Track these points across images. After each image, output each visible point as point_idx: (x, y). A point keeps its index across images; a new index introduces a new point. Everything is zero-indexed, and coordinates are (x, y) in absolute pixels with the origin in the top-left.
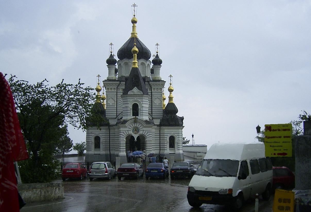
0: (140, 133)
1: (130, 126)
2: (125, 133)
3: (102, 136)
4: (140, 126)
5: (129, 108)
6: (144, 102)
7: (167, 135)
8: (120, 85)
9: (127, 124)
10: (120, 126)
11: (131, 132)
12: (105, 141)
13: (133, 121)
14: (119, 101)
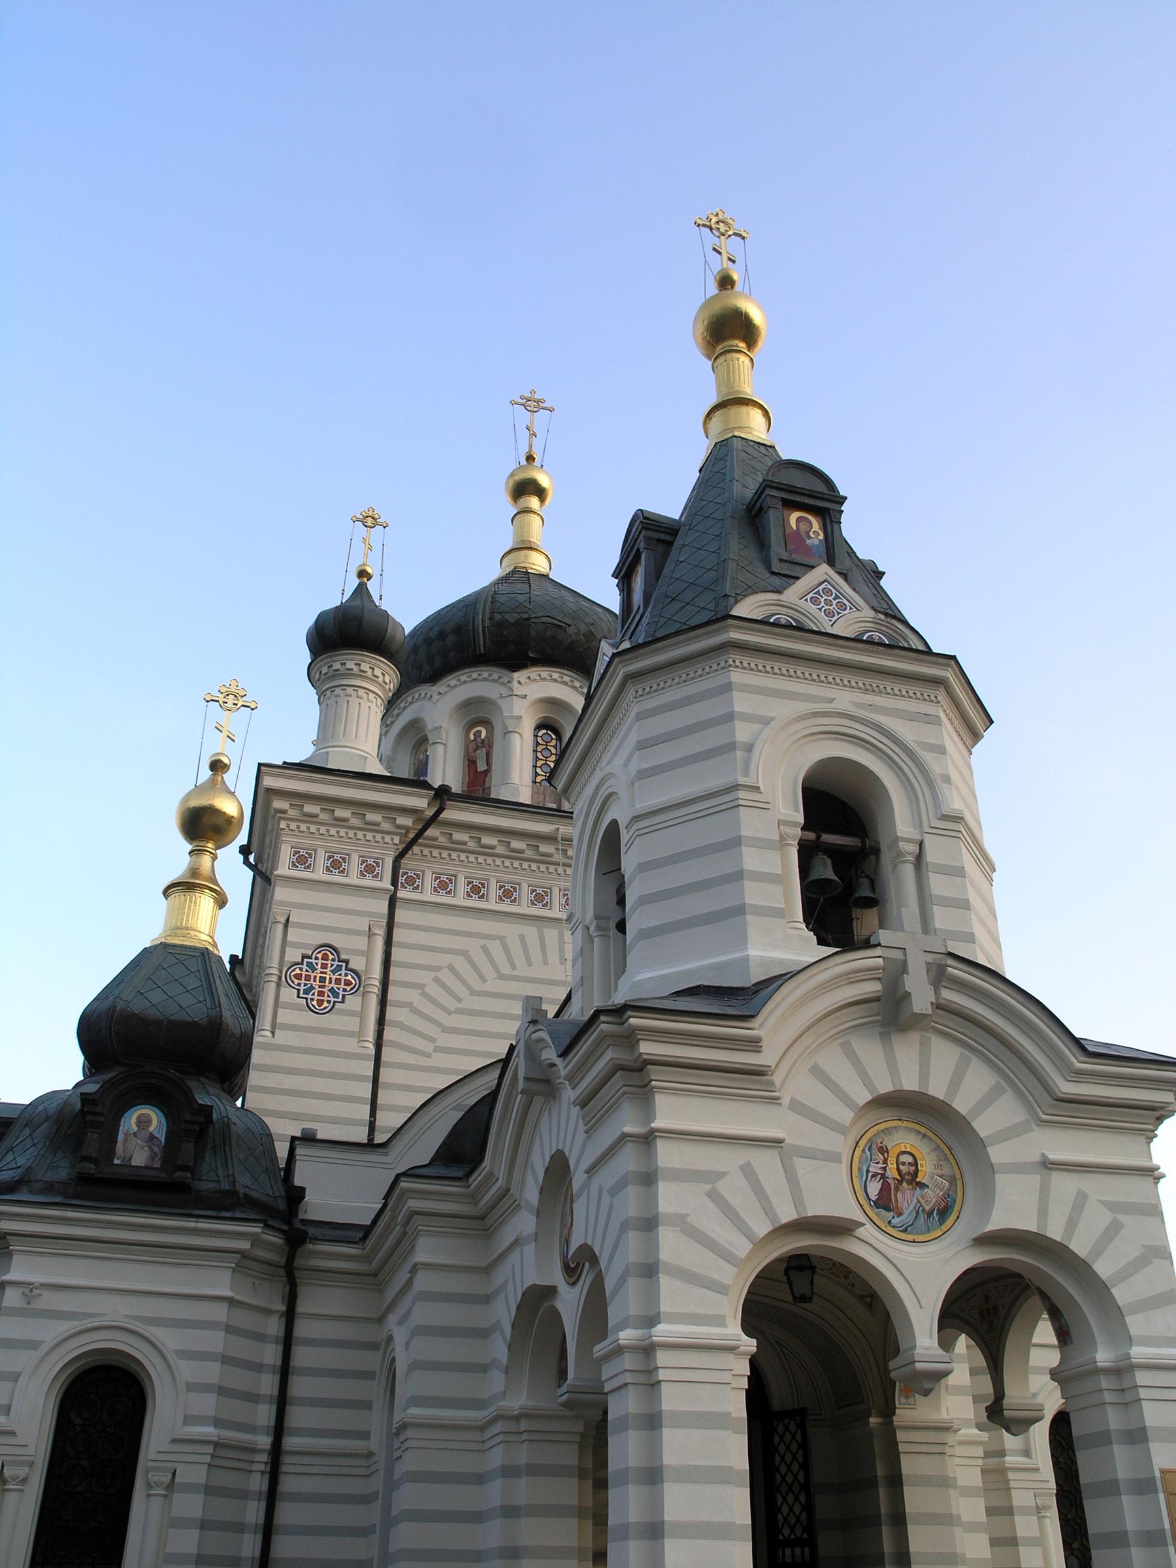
0: (998, 1221)
2: (735, 1190)
3: (183, 1354)
5: (764, 807)
8: (431, 832)
9: (776, 1026)
10: (647, 1048)
11: (832, 1193)
12: (217, 1445)
13: (873, 988)
14: (413, 996)
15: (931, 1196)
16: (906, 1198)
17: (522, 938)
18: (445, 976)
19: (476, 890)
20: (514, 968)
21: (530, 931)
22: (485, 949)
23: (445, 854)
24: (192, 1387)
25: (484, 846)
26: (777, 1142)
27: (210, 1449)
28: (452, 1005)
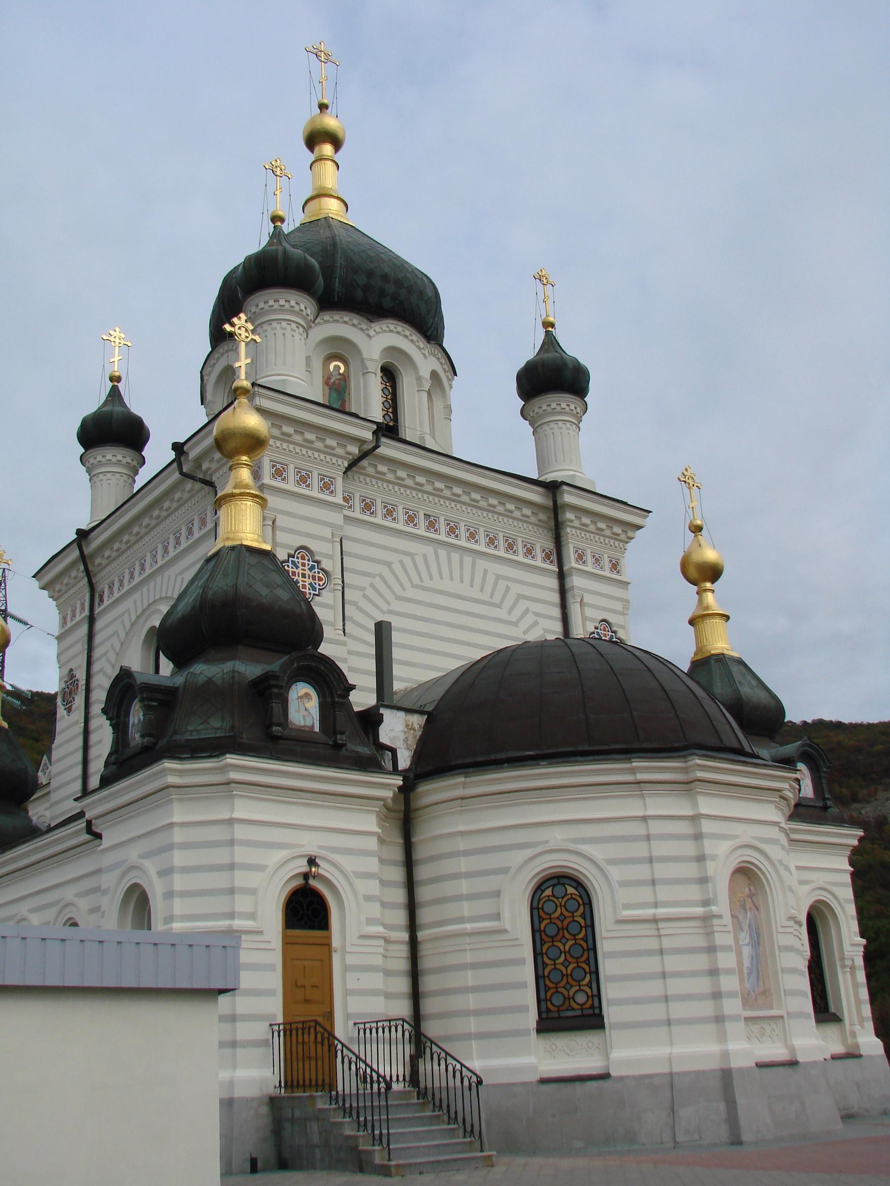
8: (364, 463)
17: (425, 556)
18: (377, 581)
19: (389, 513)
20: (422, 581)
21: (429, 550)
22: (401, 562)
23: (368, 480)
24: (368, 898)
25: (378, 472)
27: (382, 943)
28: (385, 607)
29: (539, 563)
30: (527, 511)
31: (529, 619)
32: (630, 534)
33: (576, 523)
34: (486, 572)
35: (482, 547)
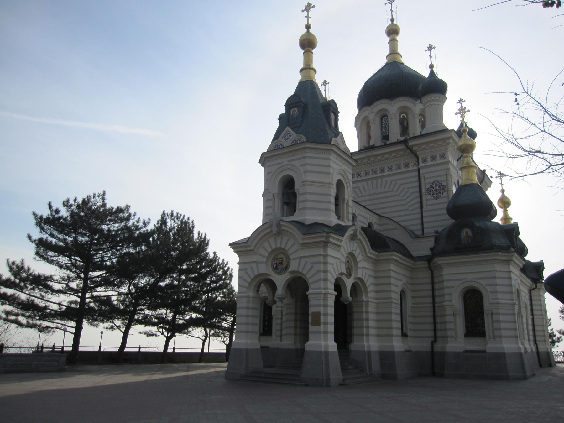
1: (263, 247)
4: (290, 244)
6: (309, 168)
7: (453, 287)
15: (284, 266)
16: (280, 267)
17: (363, 186)
20: (361, 193)
21: (365, 183)
26: (255, 262)
29: (411, 168)
30: (401, 153)
31: (406, 190)
32: (447, 141)
33: (419, 149)
34: (387, 181)
35: (386, 173)
